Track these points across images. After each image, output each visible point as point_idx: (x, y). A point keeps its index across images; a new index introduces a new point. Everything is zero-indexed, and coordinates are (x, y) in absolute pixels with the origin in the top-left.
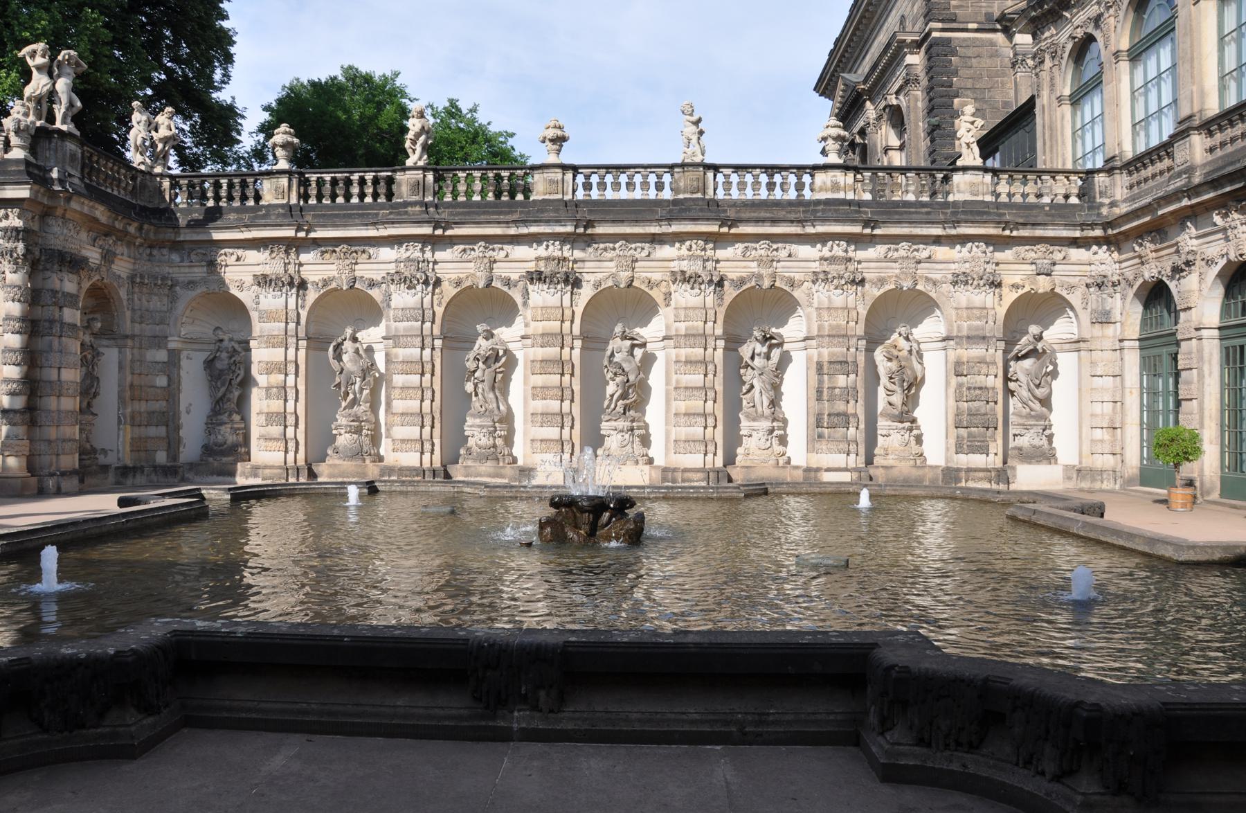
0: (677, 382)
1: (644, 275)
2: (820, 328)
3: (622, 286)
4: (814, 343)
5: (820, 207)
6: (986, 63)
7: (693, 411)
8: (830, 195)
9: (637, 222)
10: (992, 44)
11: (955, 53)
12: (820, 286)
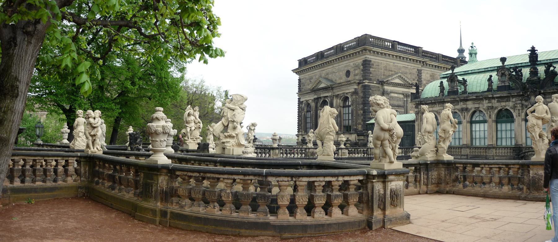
11: (370, 89)
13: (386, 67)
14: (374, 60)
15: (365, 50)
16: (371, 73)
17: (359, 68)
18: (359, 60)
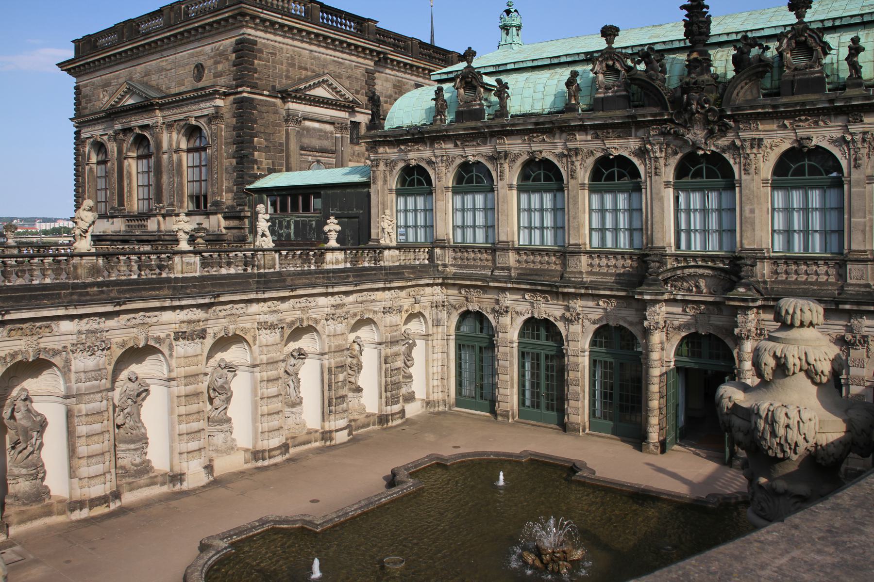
0: (262, 394)
1: (242, 325)
2: (330, 347)
3: (230, 335)
4: (326, 356)
5: (331, 275)
6: (272, 117)
7: (272, 412)
8: (335, 267)
9: (244, 292)
10: (275, 105)
11: (255, 108)
12: (330, 322)
13: (293, 58)
14: (263, 41)
15: (243, 15)
16: (255, 71)
17: (227, 59)
18: (227, 42)
